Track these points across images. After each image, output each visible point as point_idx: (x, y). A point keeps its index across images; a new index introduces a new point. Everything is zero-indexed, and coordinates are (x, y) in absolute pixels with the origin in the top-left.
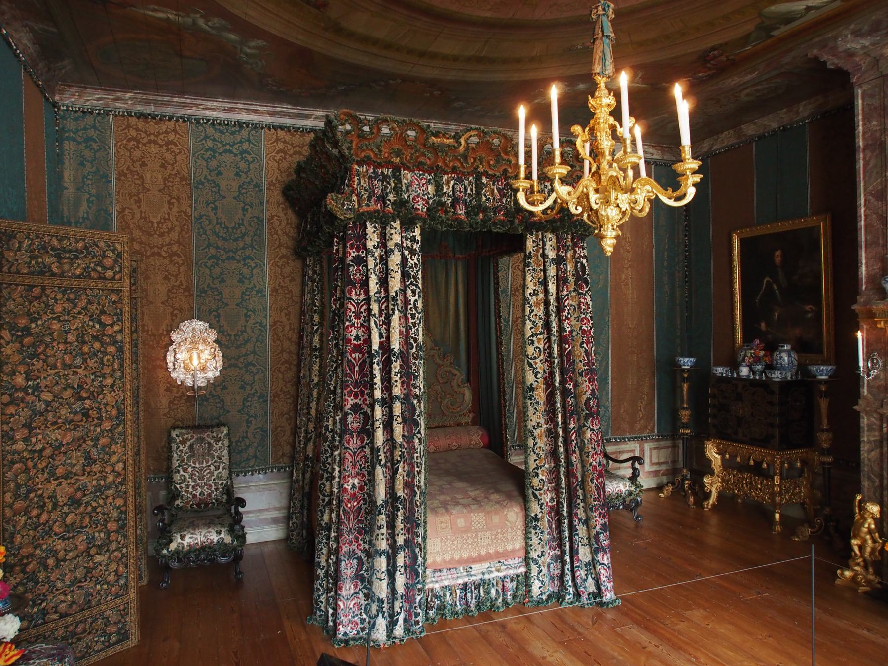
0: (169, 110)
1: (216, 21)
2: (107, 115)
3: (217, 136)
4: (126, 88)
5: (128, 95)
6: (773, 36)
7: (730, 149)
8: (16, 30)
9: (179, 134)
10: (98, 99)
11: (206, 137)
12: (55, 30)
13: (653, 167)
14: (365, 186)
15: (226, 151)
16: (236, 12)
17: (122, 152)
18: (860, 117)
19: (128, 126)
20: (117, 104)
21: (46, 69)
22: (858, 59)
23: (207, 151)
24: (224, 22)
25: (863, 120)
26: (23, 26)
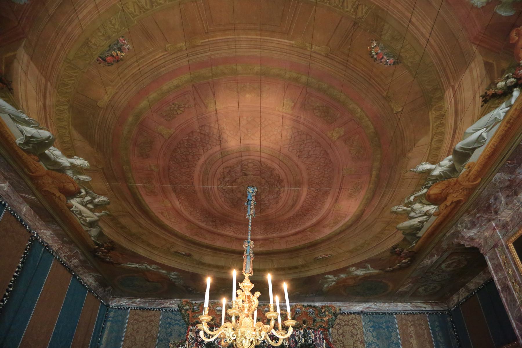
0: (154, 306)
1: (154, 266)
2: (128, 309)
3: (173, 317)
4: (136, 297)
5: (138, 300)
6: (420, 238)
7: (467, 299)
8: (86, 277)
9: (156, 316)
10: (126, 303)
11: (168, 317)
12: (100, 275)
13: (427, 315)
14: (193, 336)
15: (176, 324)
16: (159, 262)
17: (130, 326)
18: (493, 272)
19: (136, 314)
20: (133, 304)
21: (103, 291)
22: (477, 240)
23: (167, 324)
24: (156, 266)
25: (495, 273)
26: (89, 275)
